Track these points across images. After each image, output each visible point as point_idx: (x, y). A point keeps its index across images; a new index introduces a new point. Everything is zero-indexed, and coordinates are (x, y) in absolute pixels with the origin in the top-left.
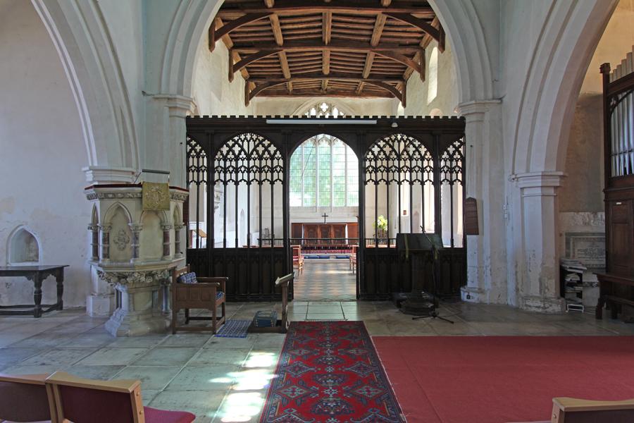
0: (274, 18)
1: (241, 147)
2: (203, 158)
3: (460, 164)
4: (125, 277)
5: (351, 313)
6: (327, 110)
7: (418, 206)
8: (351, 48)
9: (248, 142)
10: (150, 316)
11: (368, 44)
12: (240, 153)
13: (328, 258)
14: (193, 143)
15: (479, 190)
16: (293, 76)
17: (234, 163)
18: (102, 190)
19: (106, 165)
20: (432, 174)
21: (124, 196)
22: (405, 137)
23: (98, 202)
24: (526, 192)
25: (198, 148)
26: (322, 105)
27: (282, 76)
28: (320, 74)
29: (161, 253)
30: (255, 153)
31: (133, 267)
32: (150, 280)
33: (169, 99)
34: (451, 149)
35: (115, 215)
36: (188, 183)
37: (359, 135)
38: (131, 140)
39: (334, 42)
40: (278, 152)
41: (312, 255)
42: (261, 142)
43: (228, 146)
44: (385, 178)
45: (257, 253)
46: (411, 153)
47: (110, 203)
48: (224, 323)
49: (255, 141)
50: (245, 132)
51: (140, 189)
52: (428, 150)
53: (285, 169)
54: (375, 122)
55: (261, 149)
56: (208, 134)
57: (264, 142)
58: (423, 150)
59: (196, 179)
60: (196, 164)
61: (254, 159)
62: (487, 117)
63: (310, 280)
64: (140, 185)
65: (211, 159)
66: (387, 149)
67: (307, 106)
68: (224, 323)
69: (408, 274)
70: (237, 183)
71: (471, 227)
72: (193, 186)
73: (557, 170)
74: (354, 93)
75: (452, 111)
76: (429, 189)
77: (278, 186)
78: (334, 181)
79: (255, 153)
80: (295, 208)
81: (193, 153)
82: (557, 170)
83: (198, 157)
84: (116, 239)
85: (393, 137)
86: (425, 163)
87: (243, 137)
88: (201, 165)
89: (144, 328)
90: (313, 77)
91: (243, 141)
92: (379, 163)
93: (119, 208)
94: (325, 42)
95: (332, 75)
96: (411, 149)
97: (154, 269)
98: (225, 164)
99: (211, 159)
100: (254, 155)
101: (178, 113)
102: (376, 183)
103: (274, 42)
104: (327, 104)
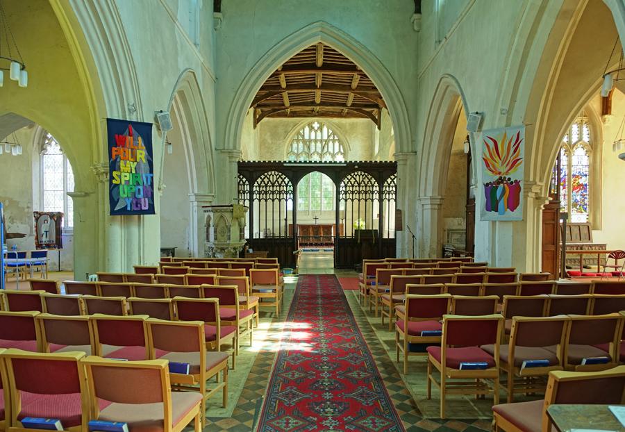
0: (282, 76)
1: (269, 179)
3: (394, 189)
4: (224, 250)
5: (332, 272)
6: (318, 128)
7: (381, 214)
8: (336, 89)
9: (273, 176)
11: (349, 88)
12: (268, 183)
13: (318, 250)
15: (403, 204)
17: (264, 189)
19: (202, 193)
20: (378, 195)
21: (226, 211)
22: (363, 173)
23: (211, 214)
24: (425, 207)
25: (244, 180)
27: (283, 105)
28: (313, 103)
31: (229, 244)
33: (229, 152)
34: (389, 180)
37: (337, 172)
39: (323, 86)
41: (306, 249)
42: (280, 176)
44: (351, 197)
45: (278, 241)
46: (366, 183)
47: (217, 214)
50: (271, 170)
52: (376, 181)
53: (294, 192)
54: (345, 165)
55: (280, 180)
56: (250, 172)
58: (373, 180)
62: (408, 163)
63: (306, 262)
64: (232, 206)
65: (251, 186)
66: (353, 180)
69: (360, 250)
70: (266, 200)
71: (399, 227)
73: (439, 195)
74: (340, 115)
75: (389, 157)
76: (376, 203)
78: (324, 187)
80: (301, 212)
81: (241, 183)
82: (439, 195)
85: (356, 173)
86: (374, 189)
87: (270, 173)
90: (308, 106)
92: (348, 188)
93: (222, 216)
95: (322, 104)
96: (366, 180)
97: (236, 246)
99: (251, 186)
100: (277, 184)
101: (234, 160)
102: (346, 200)
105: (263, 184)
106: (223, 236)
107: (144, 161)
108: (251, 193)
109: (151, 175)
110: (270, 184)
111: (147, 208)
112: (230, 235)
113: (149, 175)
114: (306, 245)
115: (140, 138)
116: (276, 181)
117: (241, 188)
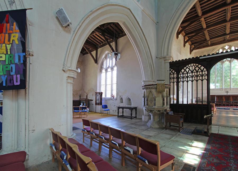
2: (175, 74)
4: (152, 111)
9: (192, 67)
10: (159, 123)
13: (229, 109)
14: (172, 70)
16: (211, 39)
17: (186, 75)
18: (146, 87)
21: (152, 88)
23: (145, 90)
25: (173, 71)
26: (225, 46)
27: (206, 40)
29: (162, 105)
30: (195, 70)
31: (154, 108)
32: (159, 113)
33: (164, 58)
35: (149, 94)
36: (170, 83)
38: (153, 72)
40: (205, 69)
43: (184, 69)
47: (148, 90)
48: (183, 129)
49: (194, 66)
50: (191, 63)
51: (156, 86)
53: (208, 75)
55: (197, 69)
57: (198, 66)
59: (173, 81)
60: (173, 77)
61: (195, 73)
64: (156, 85)
65: (178, 74)
67: (218, 49)
68: (183, 129)
72: (172, 84)
77: (205, 82)
78: (232, 77)
79: (195, 70)
81: (172, 73)
83: (173, 74)
84: (150, 100)
87: (190, 65)
88: (174, 77)
89: (157, 126)
91: (190, 67)
93: (151, 92)
94: (227, 21)
98: (183, 76)
99: (178, 74)
101: (167, 61)
103: (202, 28)
104: (228, 46)
105: (185, 72)
106: (152, 103)
107: (17, 42)
108: (178, 78)
109: (24, 54)
110: (190, 71)
111: (18, 83)
112: (155, 103)
113: (22, 55)
114: (220, 105)
115: (15, 23)
116: (195, 69)
117: (172, 76)
